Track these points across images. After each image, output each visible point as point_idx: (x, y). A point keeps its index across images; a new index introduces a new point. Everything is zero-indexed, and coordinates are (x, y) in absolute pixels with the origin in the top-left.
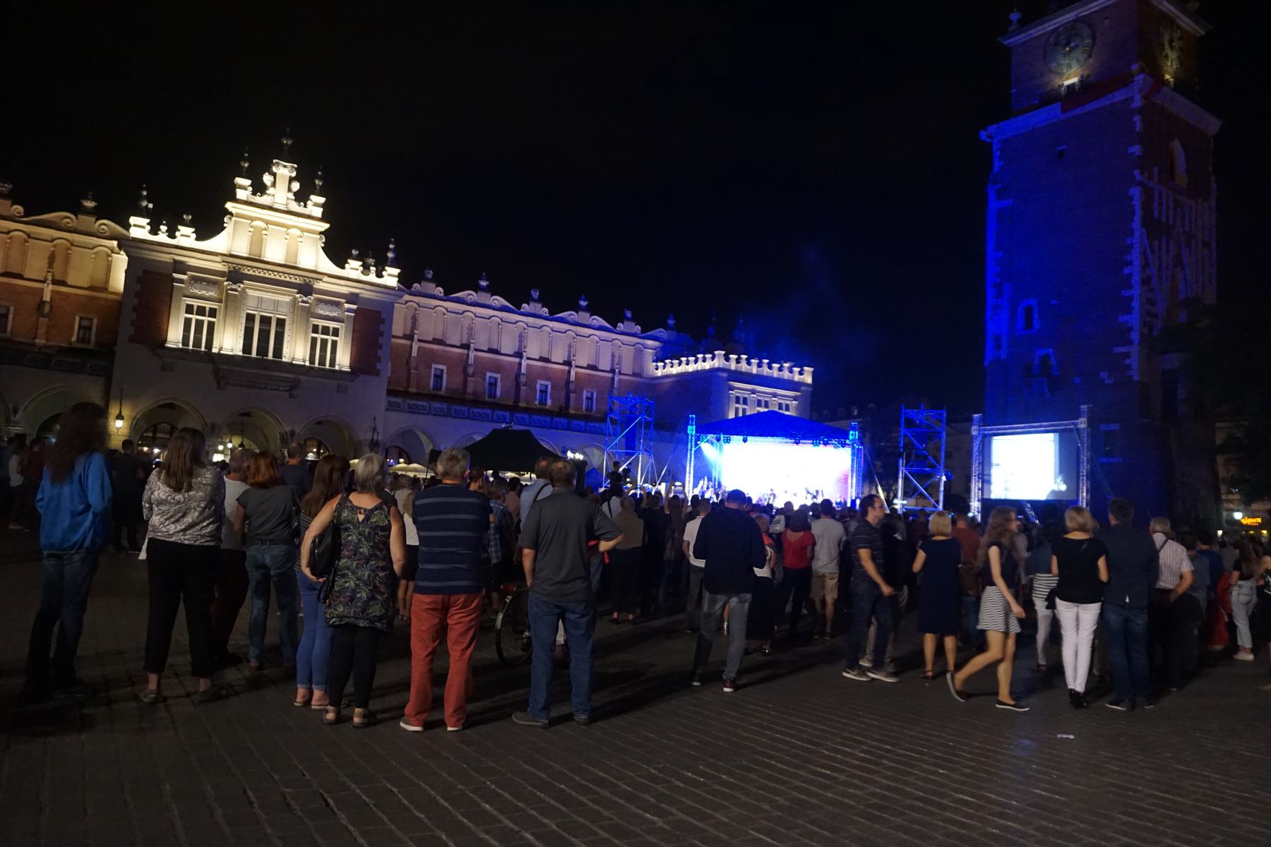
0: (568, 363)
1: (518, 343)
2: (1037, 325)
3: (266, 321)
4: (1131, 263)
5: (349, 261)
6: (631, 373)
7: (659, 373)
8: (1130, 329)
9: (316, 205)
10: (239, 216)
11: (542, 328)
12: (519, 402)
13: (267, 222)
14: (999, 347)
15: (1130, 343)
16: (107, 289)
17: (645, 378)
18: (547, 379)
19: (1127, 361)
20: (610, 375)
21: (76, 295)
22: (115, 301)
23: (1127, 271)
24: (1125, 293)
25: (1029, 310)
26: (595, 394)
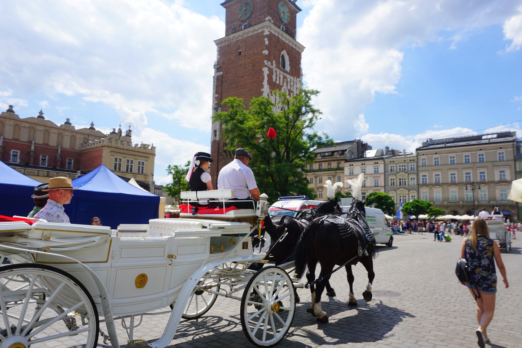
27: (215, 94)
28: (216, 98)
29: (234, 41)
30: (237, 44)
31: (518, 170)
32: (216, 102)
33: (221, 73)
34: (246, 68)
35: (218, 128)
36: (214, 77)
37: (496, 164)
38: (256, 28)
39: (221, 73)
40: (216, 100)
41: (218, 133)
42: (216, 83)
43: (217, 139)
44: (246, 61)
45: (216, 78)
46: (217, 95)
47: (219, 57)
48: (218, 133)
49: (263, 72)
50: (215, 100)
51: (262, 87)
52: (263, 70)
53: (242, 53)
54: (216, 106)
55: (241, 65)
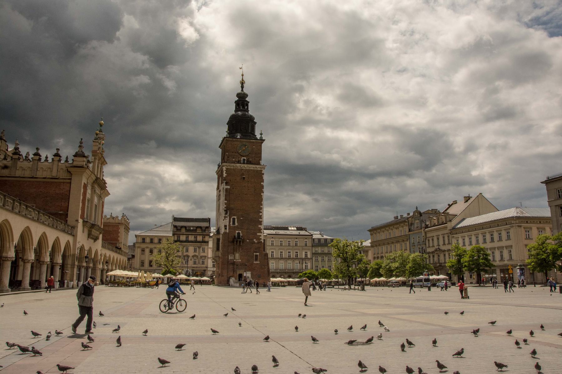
2: (236, 224)
25: (234, 219)
27: (224, 200)
28: (225, 203)
29: (239, 168)
30: (241, 171)
31: (313, 252)
32: (225, 206)
33: (229, 187)
34: (249, 190)
35: (228, 224)
37: (304, 248)
38: (257, 167)
40: (225, 205)
43: (227, 231)
44: (249, 185)
50: (224, 204)
52: (262, 194)
53: (246, 179)
54: (225, 209)
55: (245, 186)
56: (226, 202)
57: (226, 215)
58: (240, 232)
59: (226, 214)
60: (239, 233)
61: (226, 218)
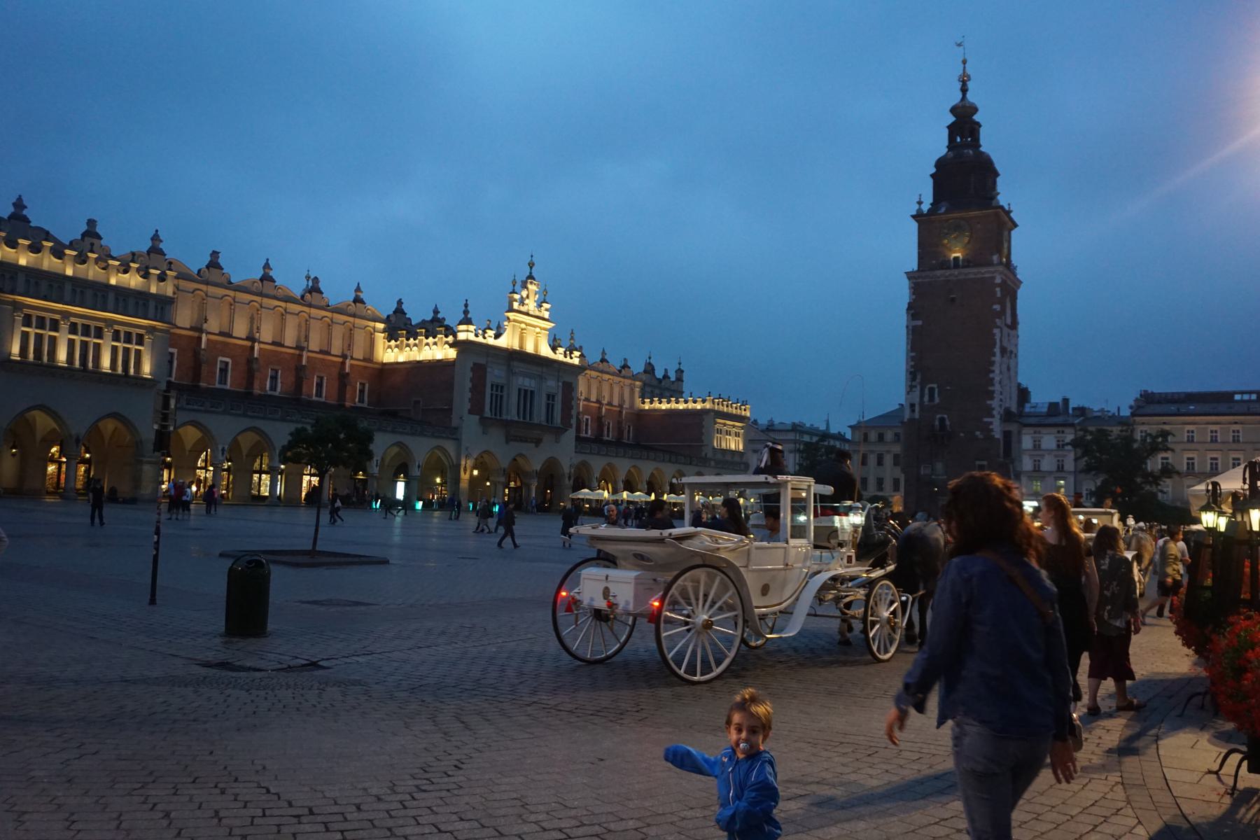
0: (199, 329)
1: (296, 333)
2: (937, 400)
3: (526, 391)
4: (993, 372)
5: (574, 352)
6: (361, 358)
7: (647, 407)
8: (993, 409)
9: (547, 310)
10: (515, 321)
11: (300, 314)
12: (199, 381)
13: (526, 324)
14: (913, 411)
15: (993, 416)
16: (372, 361)
17: (376, 363)
18: (589, 415)
19: (991, 427)
20: (340, 360)
21: (358, 365)
22: (373, 368)
23: (991, 375)
24: (990, 388)
25: (932, 390)
26: (367, 385)
32: (913, 363)
33: (920, 323)
35: (917, 400)
36: (907, 327)
39: (920, 323)
40: (912, 360)
41: (917, 408)
42: (911, 337)
43: (917, 415)
45: (910, 328)
46: (913, 354)
47: (914, 297)
48: (917, 408)
49: (994, 335)
50: (909, 360)
51: (994, 355)
54: (912, 370)
56: (913, 354)
57: (914, 383)
58: (946, 416)
59: (913, 379)
60: (942, 420)
61: (914, 389)
